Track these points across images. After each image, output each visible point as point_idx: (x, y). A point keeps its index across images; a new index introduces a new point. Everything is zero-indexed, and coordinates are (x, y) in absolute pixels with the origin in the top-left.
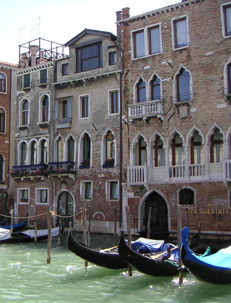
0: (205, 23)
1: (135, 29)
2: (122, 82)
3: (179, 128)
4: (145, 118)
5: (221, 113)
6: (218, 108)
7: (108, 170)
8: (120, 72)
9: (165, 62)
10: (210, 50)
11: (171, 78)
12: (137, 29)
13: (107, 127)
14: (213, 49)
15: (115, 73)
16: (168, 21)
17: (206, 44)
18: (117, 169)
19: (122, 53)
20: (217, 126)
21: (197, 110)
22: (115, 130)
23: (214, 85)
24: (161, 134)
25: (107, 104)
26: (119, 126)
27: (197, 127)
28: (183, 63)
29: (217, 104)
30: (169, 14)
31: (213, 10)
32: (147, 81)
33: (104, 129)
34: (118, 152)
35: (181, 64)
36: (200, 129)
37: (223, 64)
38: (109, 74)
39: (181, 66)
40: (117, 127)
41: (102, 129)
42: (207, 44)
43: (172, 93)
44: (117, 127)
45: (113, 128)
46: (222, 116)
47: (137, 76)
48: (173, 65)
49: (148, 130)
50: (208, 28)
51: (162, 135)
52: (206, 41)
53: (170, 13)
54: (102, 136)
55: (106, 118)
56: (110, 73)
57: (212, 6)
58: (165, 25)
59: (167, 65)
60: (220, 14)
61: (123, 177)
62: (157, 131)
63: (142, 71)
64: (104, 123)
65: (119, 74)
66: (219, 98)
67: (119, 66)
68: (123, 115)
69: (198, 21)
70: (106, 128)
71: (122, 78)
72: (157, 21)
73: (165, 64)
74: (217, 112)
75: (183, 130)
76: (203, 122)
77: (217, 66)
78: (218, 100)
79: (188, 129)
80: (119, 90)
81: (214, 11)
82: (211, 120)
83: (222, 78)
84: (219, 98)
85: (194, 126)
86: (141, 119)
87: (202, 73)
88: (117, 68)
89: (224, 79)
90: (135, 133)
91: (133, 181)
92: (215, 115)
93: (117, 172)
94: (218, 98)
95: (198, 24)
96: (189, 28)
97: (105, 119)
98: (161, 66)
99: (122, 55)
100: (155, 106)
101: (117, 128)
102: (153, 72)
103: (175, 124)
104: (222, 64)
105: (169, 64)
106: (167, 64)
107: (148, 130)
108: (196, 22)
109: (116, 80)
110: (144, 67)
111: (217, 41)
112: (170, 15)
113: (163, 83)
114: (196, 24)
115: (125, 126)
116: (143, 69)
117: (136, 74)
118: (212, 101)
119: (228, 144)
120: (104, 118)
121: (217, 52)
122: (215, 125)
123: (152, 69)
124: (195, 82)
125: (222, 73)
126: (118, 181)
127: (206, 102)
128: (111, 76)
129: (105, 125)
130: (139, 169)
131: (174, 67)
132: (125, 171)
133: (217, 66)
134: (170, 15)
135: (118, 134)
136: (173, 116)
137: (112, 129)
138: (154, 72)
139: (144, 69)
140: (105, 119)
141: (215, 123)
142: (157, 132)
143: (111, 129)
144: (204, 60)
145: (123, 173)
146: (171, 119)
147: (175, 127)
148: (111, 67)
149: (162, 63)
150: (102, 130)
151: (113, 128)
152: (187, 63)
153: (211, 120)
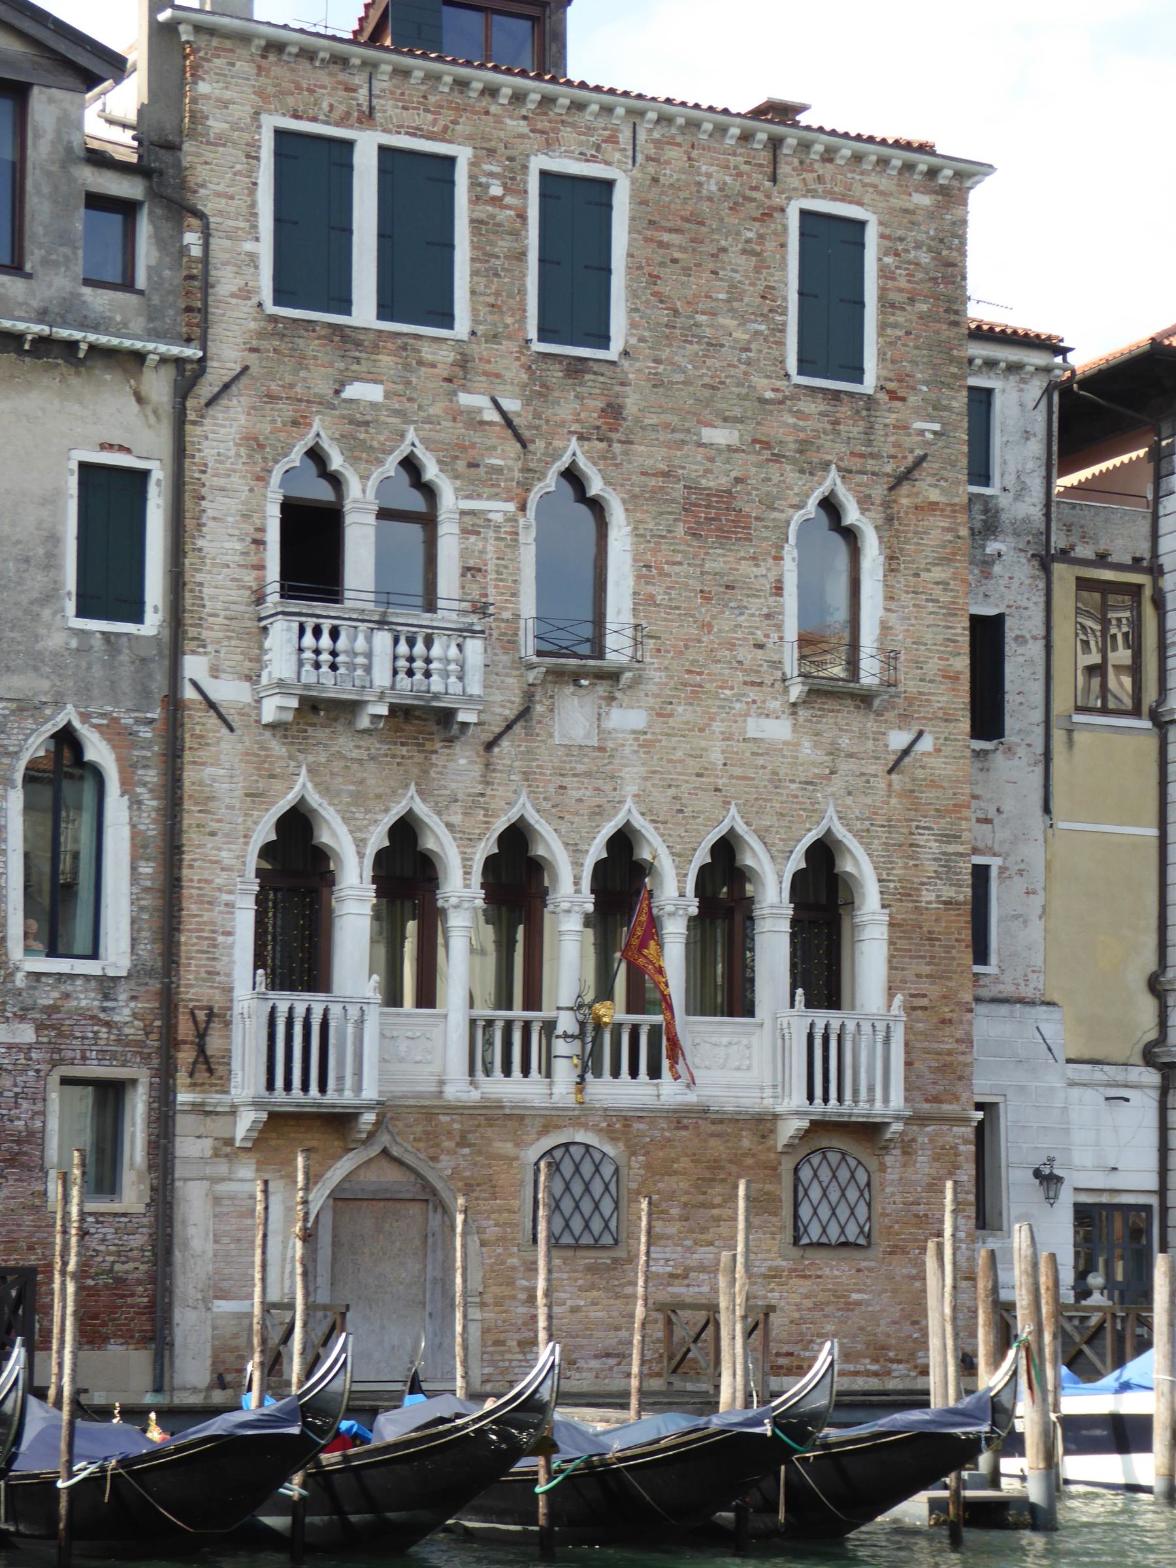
0: (711, 266)
1: (296, 116)
2: (189, 428)
3: (546, 805)
4: (384, 711)
5: (763, 767)
6: (749, 735)
7: (67, 996)
8: (179, 362)
9: (482, 401)
10: (725, 420)
11: (511, 507)
12: (314, 119)
13: (58, 704)
14: (741, 420)
15: (139, 357)
16: (511, 159)
17: (707, 380)
18: (133, 998)
19: (191, 238)
20: (741, 829)
21: (650, 727)
22: (114, 732)
23: (742, 609)
24: (439, 813)
25: (54, 539)
26: (156, 714)
27: (643, 814)
28: (581, 438)
29: (747, 715)
30: (523, 123)
31: (751, 209)
32: (364, 478)
33: (26, 707)
34: (146, 890)
35: (574, 444)
36: (656, 829)
37: (782, 516)
38: (92, 348)
39: (569, 453)
40: (138, 721)
41: (14, 705)
42: (711, 382)
43: (514, 595)
44: (138, 721)
45: (103, 715)
46: (770, 781)
47: (295, 423)
48: (526, 434)
49: (362, 782)
50: (722, 296)
51: (450, 826)
52: (709, 362)
53: (525, 118)
54: (16, 755)
55: (55, 641)
56: (104, 340)
57: (755, 188)
58: (491, 175)
59: (491, 423)
60: (783, 245)
61: (185, 1056)
62: (420, 792)
63: (334, 408)
64: (36, 669)
65: (167, 373)
66: (761, 684)
67: (153, 314)
68: (194, 652)
69: (674, 238)
70: (48, 712)
71: (190, 403)
72: (446, 128)
73: (480, 410)
74: (748, 754)
75: (567, 817)
76: (672, 792)
77: (757, 519)
78: (752, 694)
79: (599, 813)
80: (159, 474)
81: (757, 214)
82: (717, 790)
83: (779, 590)
84: (761, 684)
85: (629, 803)
86: (348, 709)
87: (680, 529)
88: (138, 324)
89: (786, 593)
90: (277, 785)
91: (288, 1086)
92: (738, 771)
93: (135, 1015)
94: (753, 683)
95: (677, 255)
96: (630, 255)
97: (39, 646)
98: (456, 414)
99: (196, 252)
100: (419, 648)
101: (142, 728)
102: (402, 435)
103: (526, 776)
104: (776, 515)
105: (508, 422)
106: (495, 417)
107: (362, 782)
108: (666, 237)
109: (140, 399)
110: (343, 385)
111: (765, 387)
112: (526, 130)
113: (467, 519)
114: (661, 244)
115: (199, 722)
116: (337, 392)
117: (288, 411)
118: (727, 692)
119: (886, 937)
120: (37, 638)
121: (760, 442)
122: (733, 819)
123: (398, 413)
124: (645, 570)
125: (778, 558)
126: (143, 1077)
127: (696, 694)
128: (100, 363)
129: (39, 685)
130: (300, 1011)
131: (531, 447)
132: (201, 1015)
133: (757, 519)
134: (523, 127)
135: (146, 767)
136: (518, 728)
137: (96, 726)
138: (411, 435)
139: (344, 395)
140: (39, 646)
141: (733, 810)
142: (417, 799)
143: (85, 717)
144: (692, 465)
145: (185, 1029)
146: (505, 743)
147: (523, 798)
148: (99, 300)
149: (464, 399)
150: (13, 712)
151: (103, 715)
152: (604, 445)
153: (717, 790)
